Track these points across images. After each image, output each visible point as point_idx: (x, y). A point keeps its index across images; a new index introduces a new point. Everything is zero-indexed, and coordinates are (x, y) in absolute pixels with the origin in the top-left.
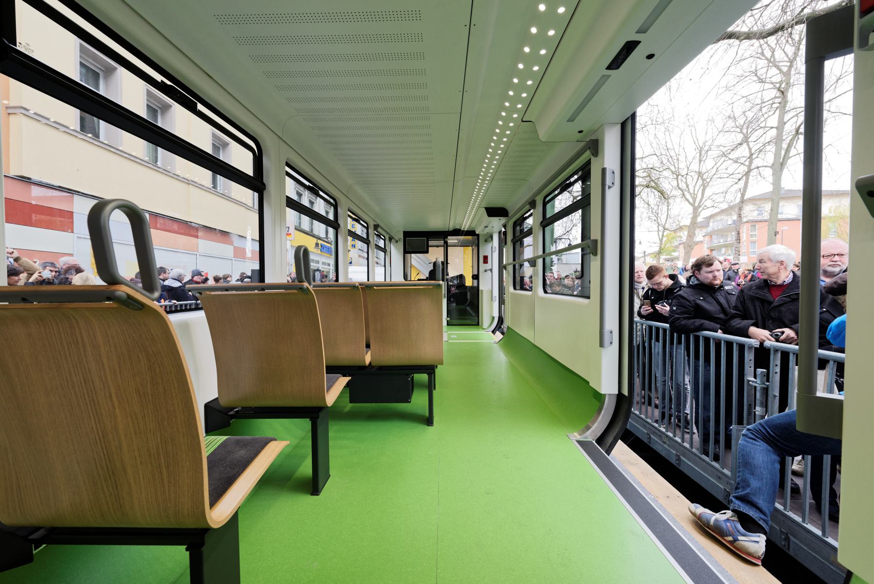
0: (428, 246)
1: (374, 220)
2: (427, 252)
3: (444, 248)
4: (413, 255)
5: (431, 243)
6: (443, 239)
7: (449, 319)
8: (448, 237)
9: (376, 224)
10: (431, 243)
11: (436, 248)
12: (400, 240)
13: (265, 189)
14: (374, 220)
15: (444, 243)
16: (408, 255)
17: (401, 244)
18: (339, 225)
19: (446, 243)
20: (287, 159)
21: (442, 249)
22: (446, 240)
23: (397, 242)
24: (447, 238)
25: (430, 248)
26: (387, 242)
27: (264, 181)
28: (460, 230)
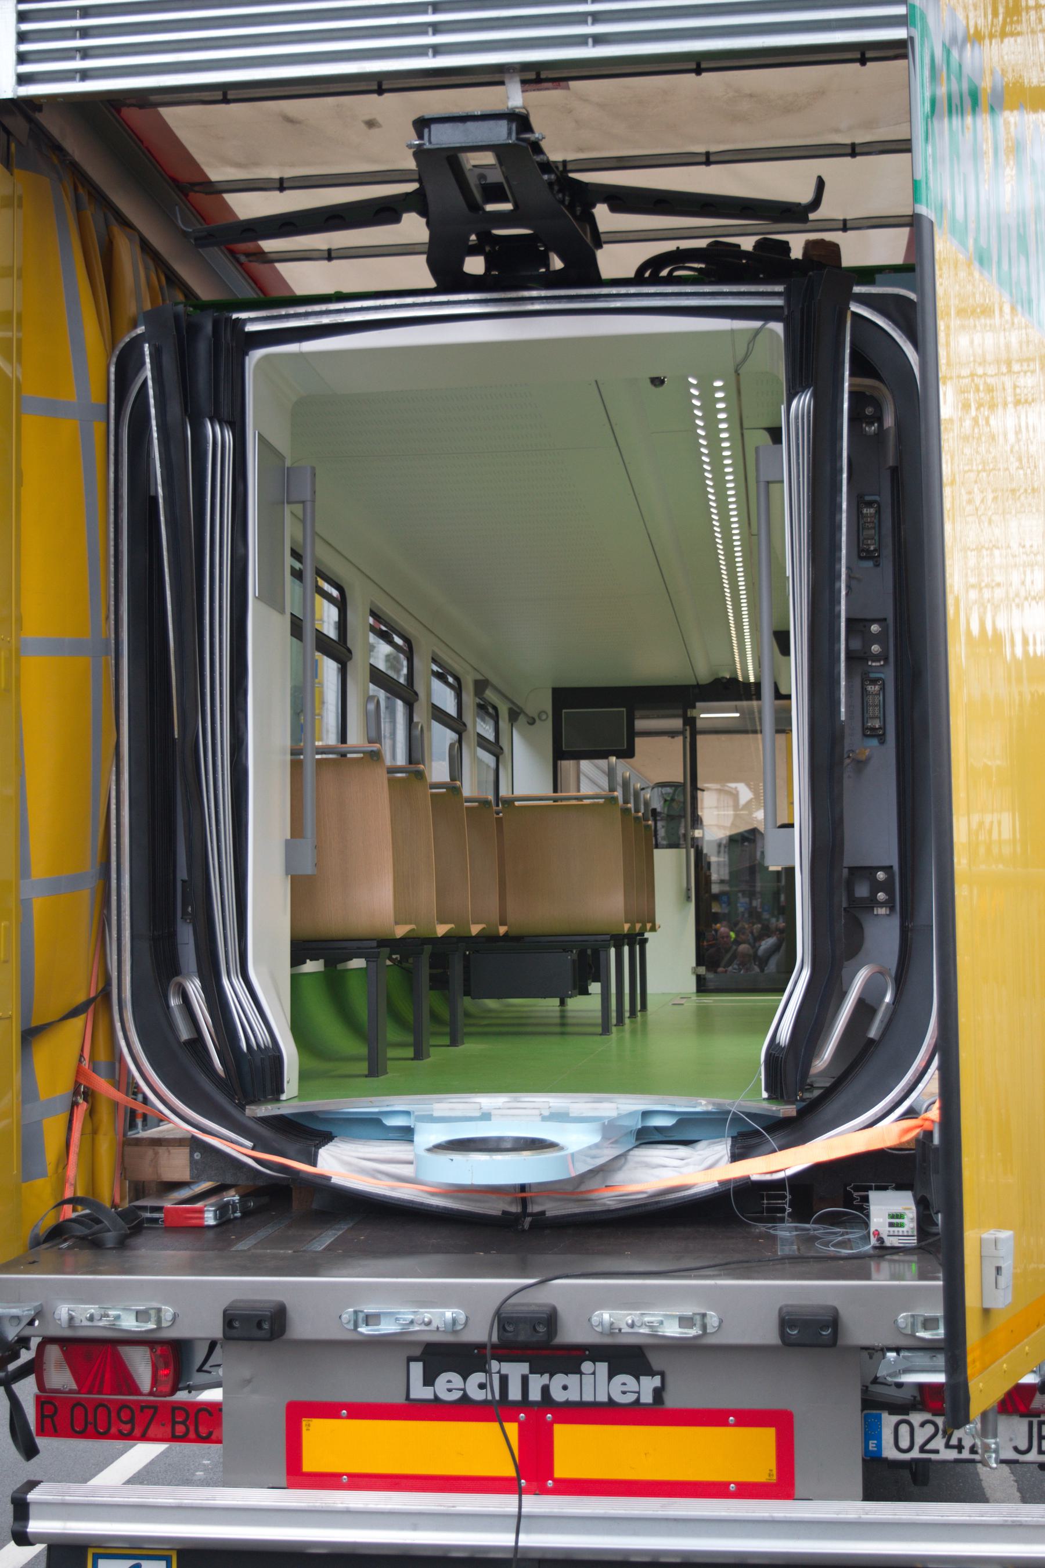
0: (632, 734)
1: (475, 669)
2: (628, 753)
3: (685, 738)
4: (585, 765)
5: (640, 724)
6: (680, 712)
7: (702, 970)
8: (698, 704)
9: (480, 677)
10: (640, 724)
11: (666, 739)
12: (544, 717)
13: (351, 659)
14: (475, 669)
15: (685, 724)
16: (567, 765)
17: (546, 728)
18: (416, 694)
19: (690, 722)
20: (372, 603)
21: (676, 746)
22: (690, 713)
23: (532, 722)
24: (694, 707)
25: (638, 741)
26: (504, 724)
27: (349, 644)
28: (734, 680)
